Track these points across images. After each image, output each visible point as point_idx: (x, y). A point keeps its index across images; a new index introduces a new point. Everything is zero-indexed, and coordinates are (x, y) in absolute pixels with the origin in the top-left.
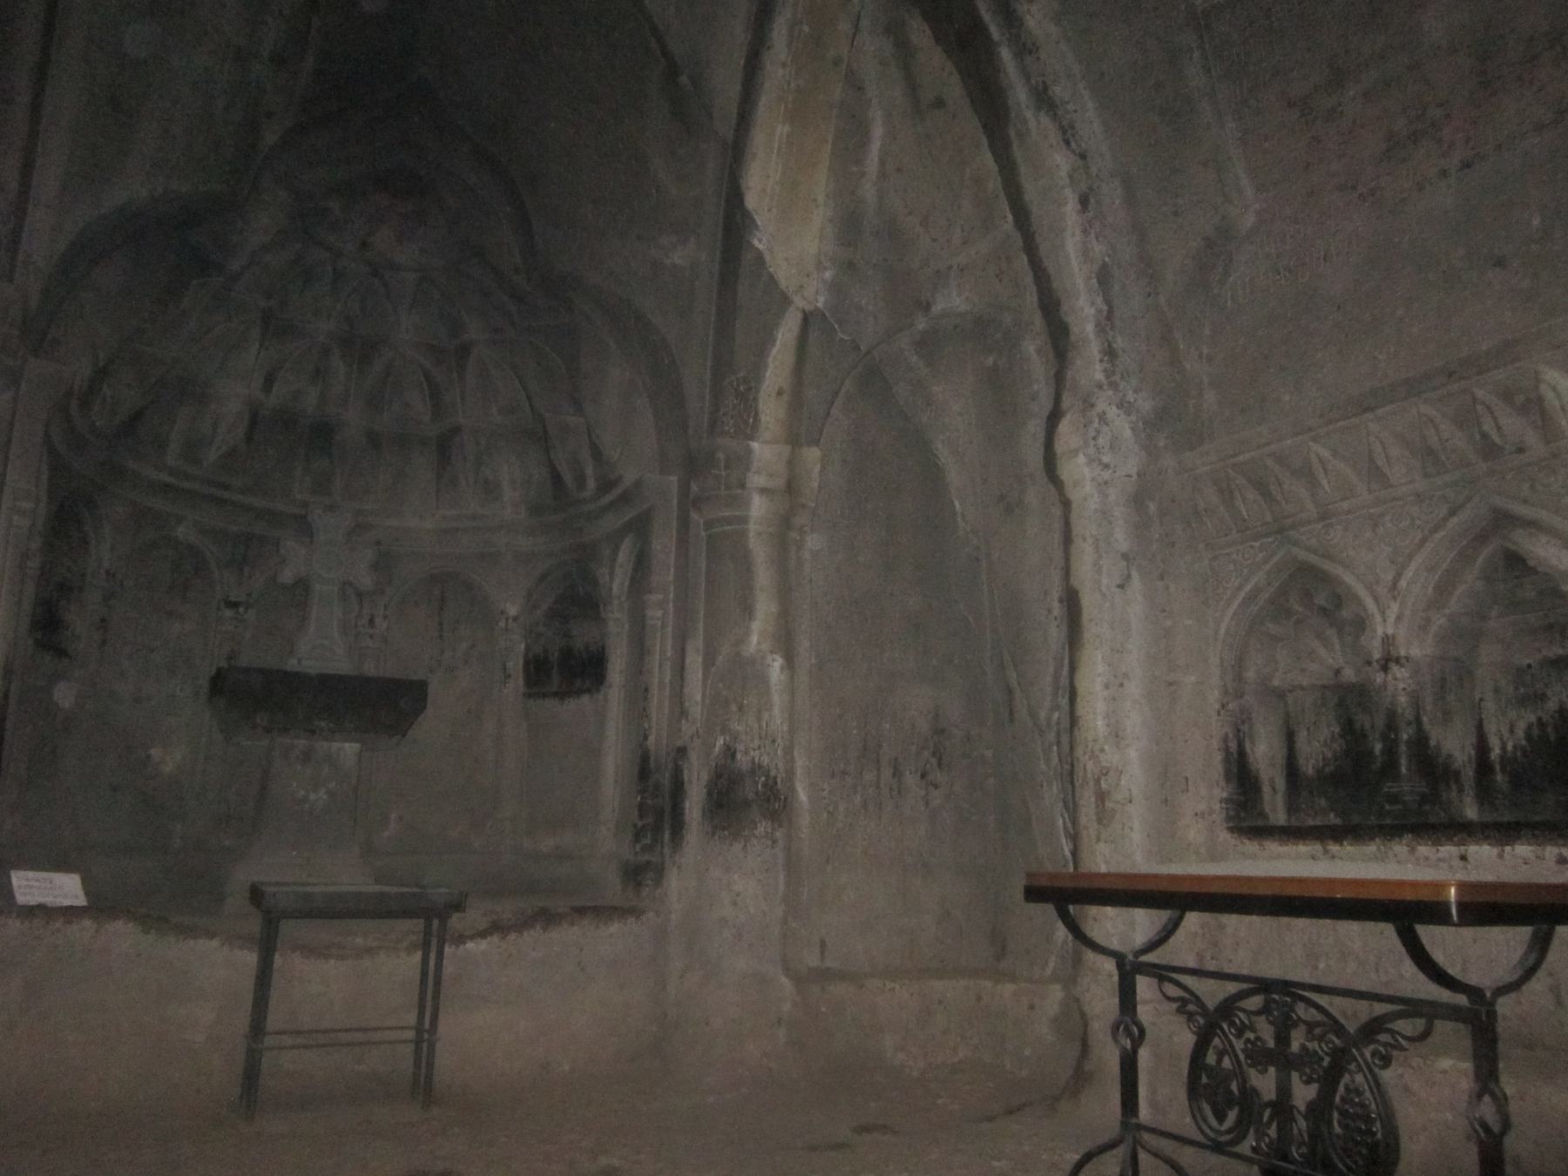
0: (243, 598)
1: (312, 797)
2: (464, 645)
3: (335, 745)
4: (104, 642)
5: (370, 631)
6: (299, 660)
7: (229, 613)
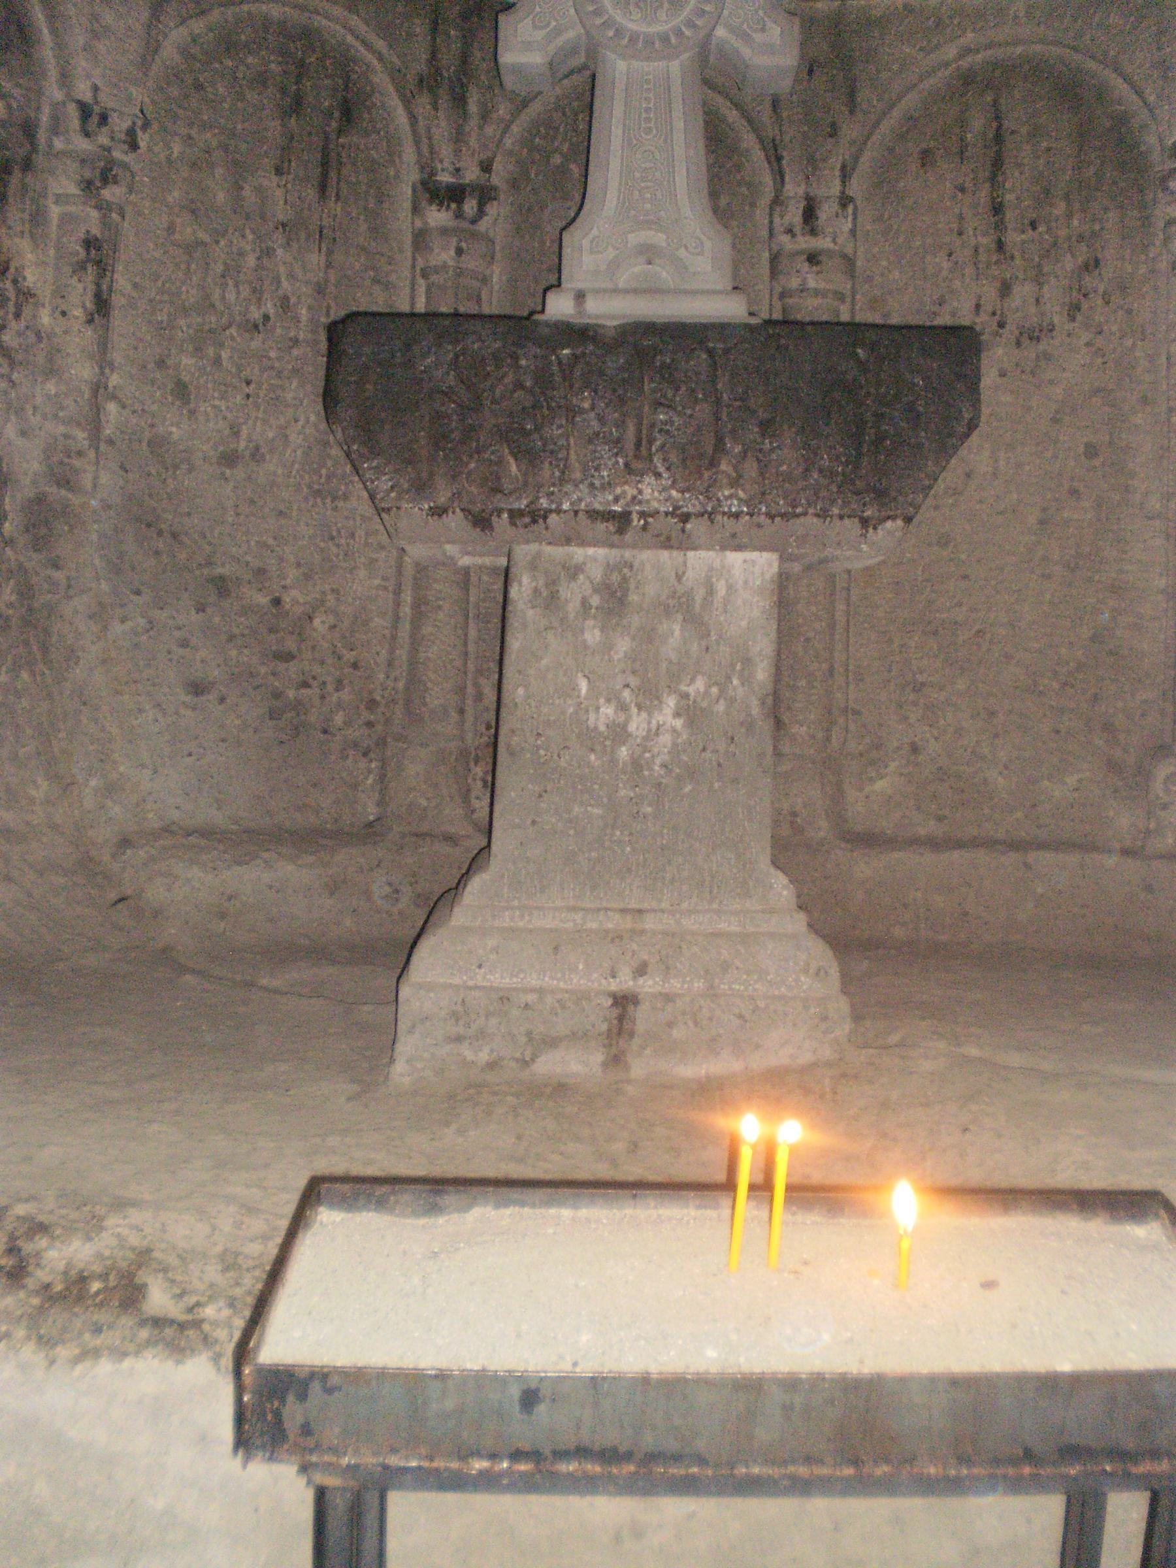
0: (472, 174)
1: (637, 724)
2: (1069, 263)
3: (699, 561)
4: (102, 305)
5: (806, 243)
6: (580, 296)
7: (437, 217)
